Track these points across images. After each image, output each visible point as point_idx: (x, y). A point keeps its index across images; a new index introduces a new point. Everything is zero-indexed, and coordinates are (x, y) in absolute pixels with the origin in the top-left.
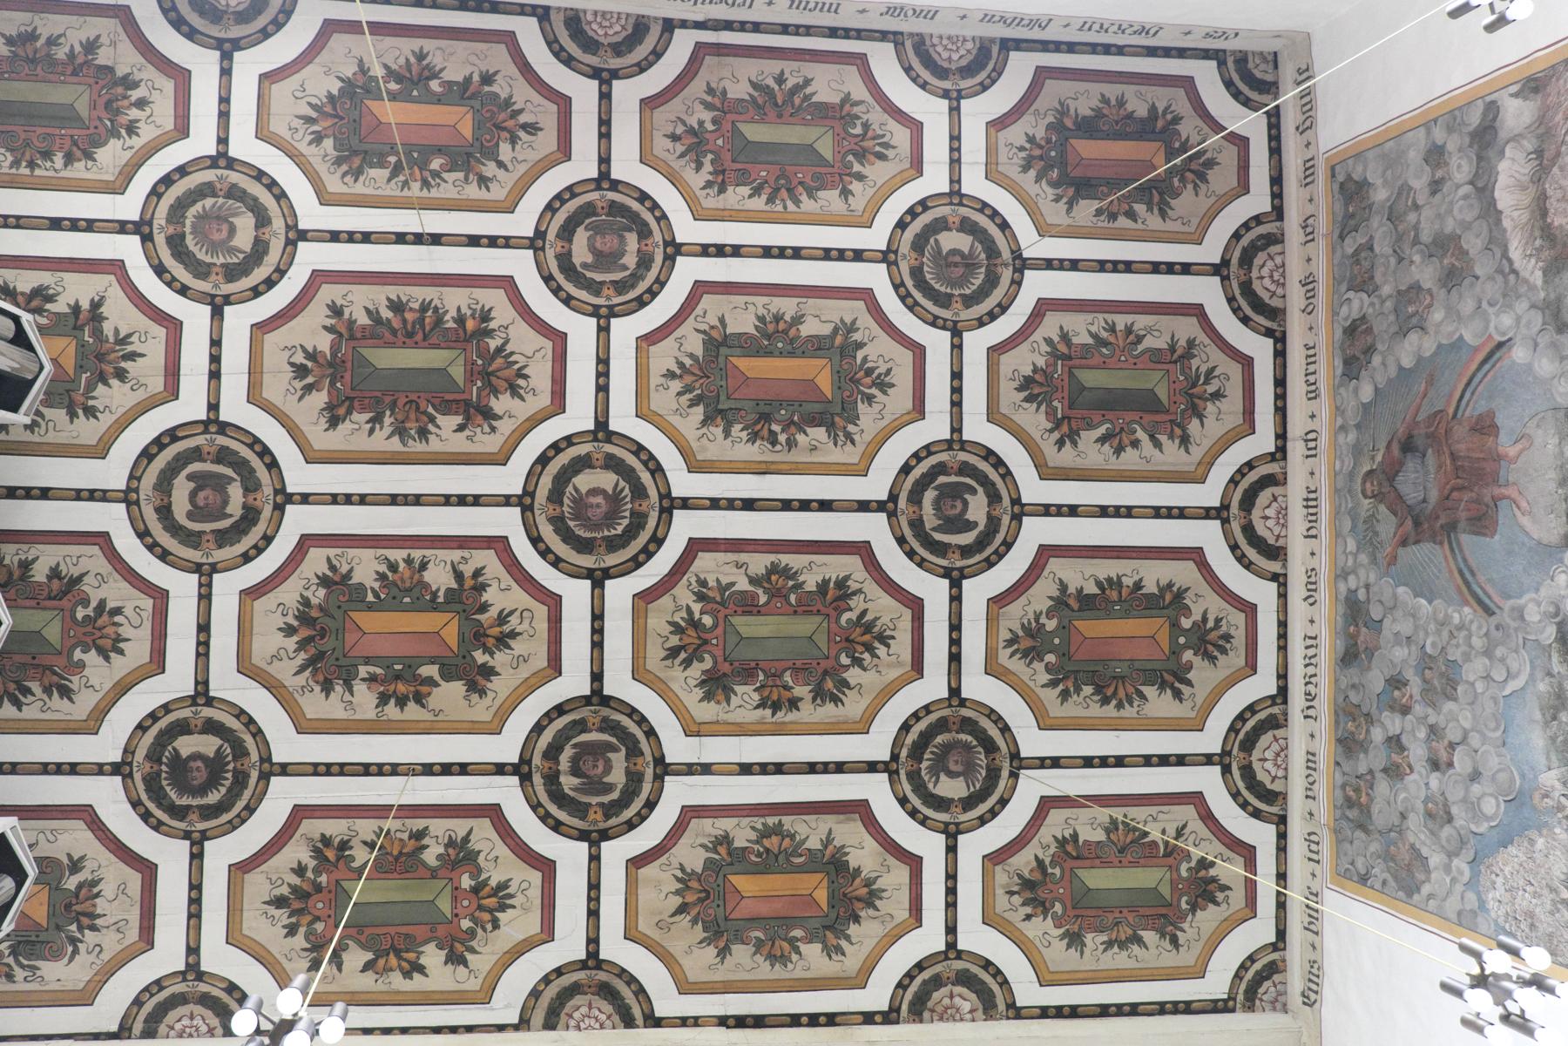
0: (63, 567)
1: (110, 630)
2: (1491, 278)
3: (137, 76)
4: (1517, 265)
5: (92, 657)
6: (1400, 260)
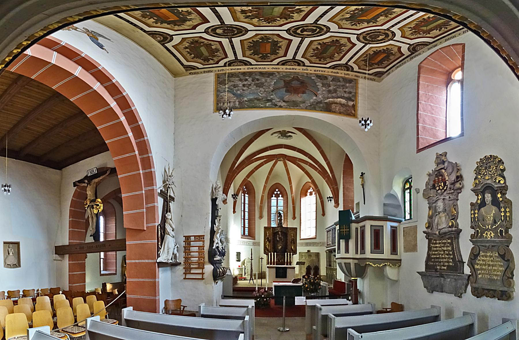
2: (328, 96)
4: (329, 99)
6: (335, 85)
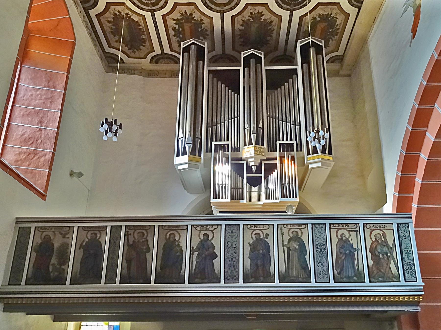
0: (241, 24)
1: (256, 15)
3: (113, 13)
5: (263, 18)
